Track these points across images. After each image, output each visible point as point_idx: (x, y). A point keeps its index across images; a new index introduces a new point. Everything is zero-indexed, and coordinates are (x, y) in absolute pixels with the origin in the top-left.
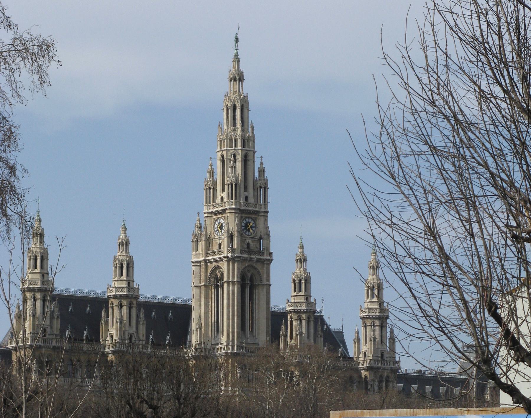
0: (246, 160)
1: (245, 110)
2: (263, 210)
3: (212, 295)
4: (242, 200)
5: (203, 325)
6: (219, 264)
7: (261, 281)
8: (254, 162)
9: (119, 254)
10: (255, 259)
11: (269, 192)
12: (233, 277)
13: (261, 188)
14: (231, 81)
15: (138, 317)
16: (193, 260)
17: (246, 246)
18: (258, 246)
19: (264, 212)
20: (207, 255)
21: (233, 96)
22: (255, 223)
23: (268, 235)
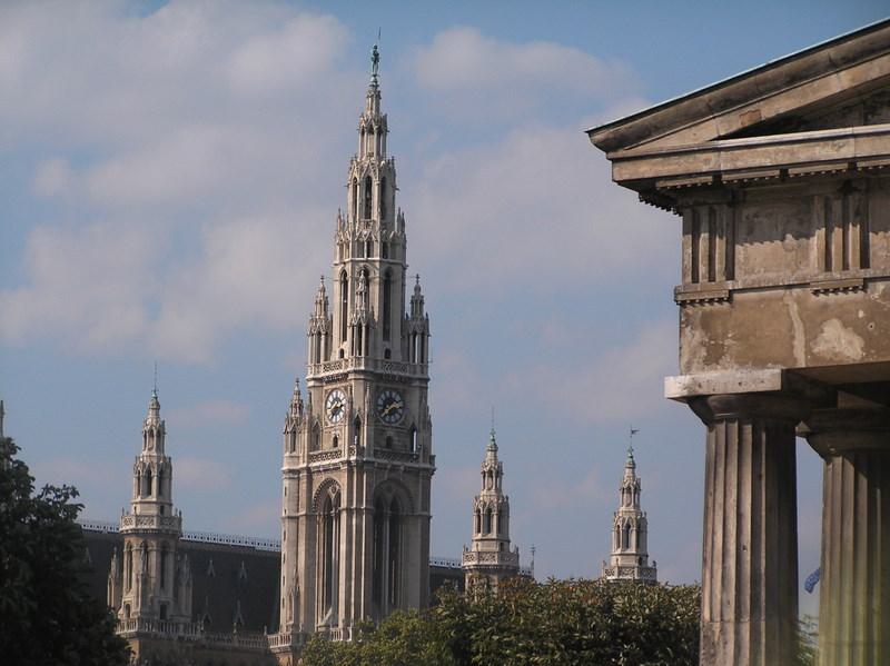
0: (388, 282)
1: (389, 189)
2: (418, 375)
3: (320, 535)
4: (381, 356)
5: (302, 589)
6: (333, 476)
7: (413, 509)
8: (403, 285)
9: (145, 453)
10: (402, 468)
11: (431, 342)
12: (359, 501)
13: (415, 334)
14: (363, 134)
15: (178, 573)
16: (285, 468)
17: (384, 443)
18: (408, 444)
19: (420, 379)
20: (311, 458)
21: (366, 163)
22: (403, 400)
23: (427, 424)
